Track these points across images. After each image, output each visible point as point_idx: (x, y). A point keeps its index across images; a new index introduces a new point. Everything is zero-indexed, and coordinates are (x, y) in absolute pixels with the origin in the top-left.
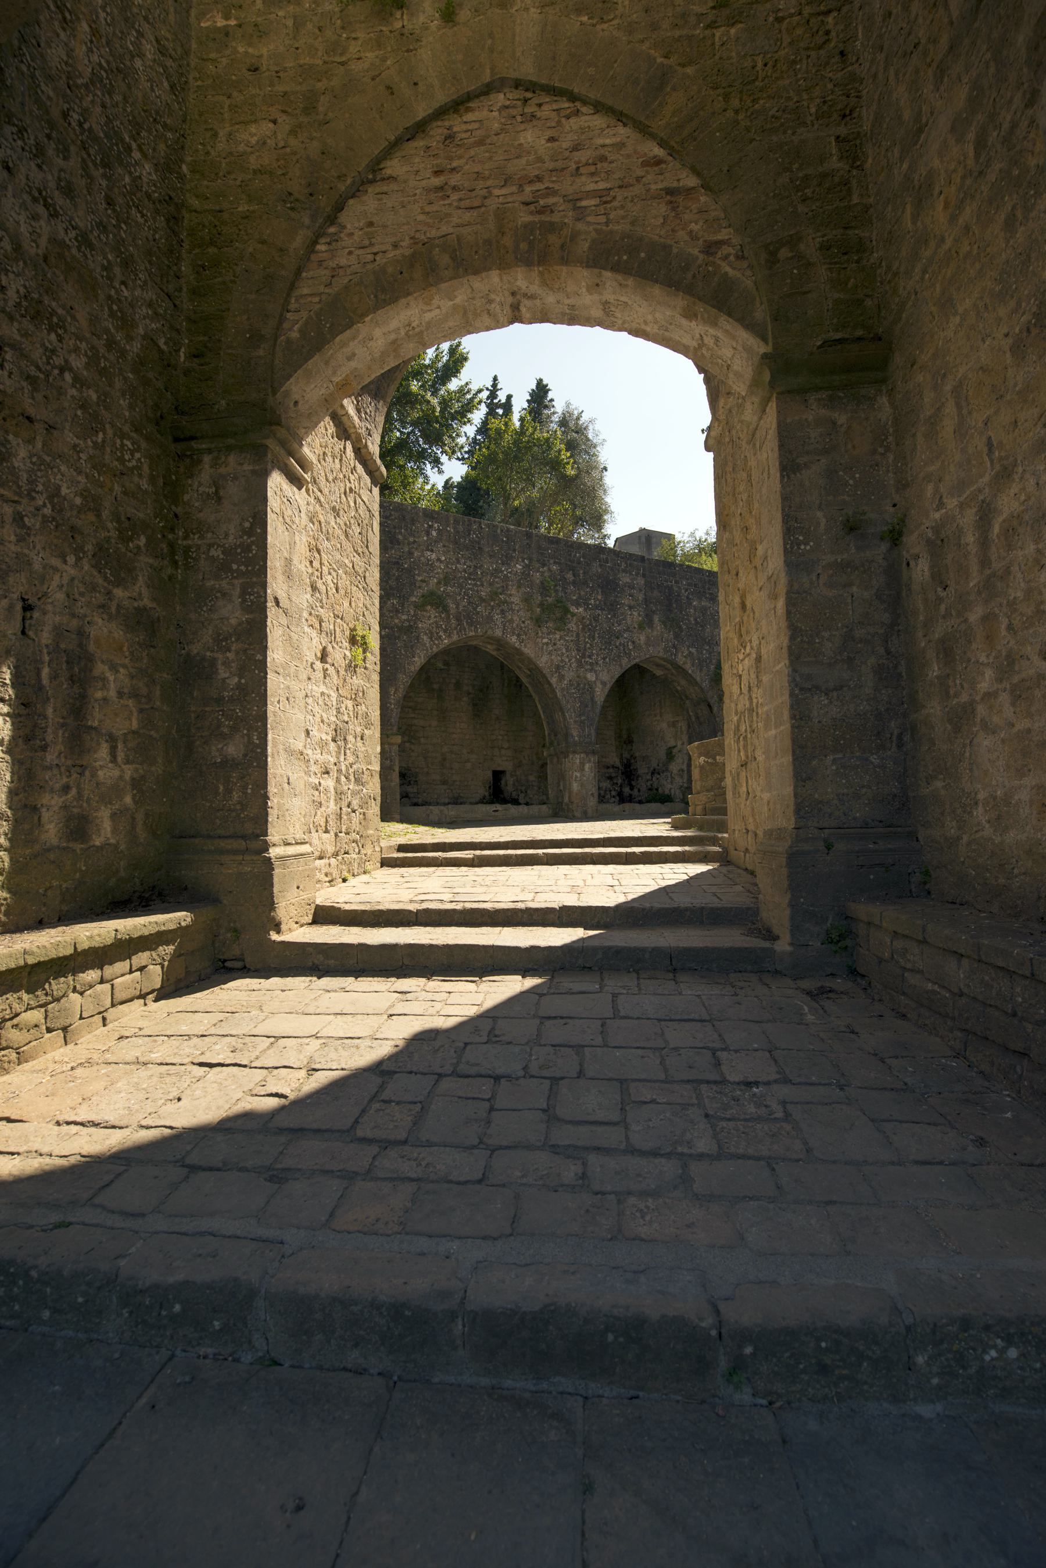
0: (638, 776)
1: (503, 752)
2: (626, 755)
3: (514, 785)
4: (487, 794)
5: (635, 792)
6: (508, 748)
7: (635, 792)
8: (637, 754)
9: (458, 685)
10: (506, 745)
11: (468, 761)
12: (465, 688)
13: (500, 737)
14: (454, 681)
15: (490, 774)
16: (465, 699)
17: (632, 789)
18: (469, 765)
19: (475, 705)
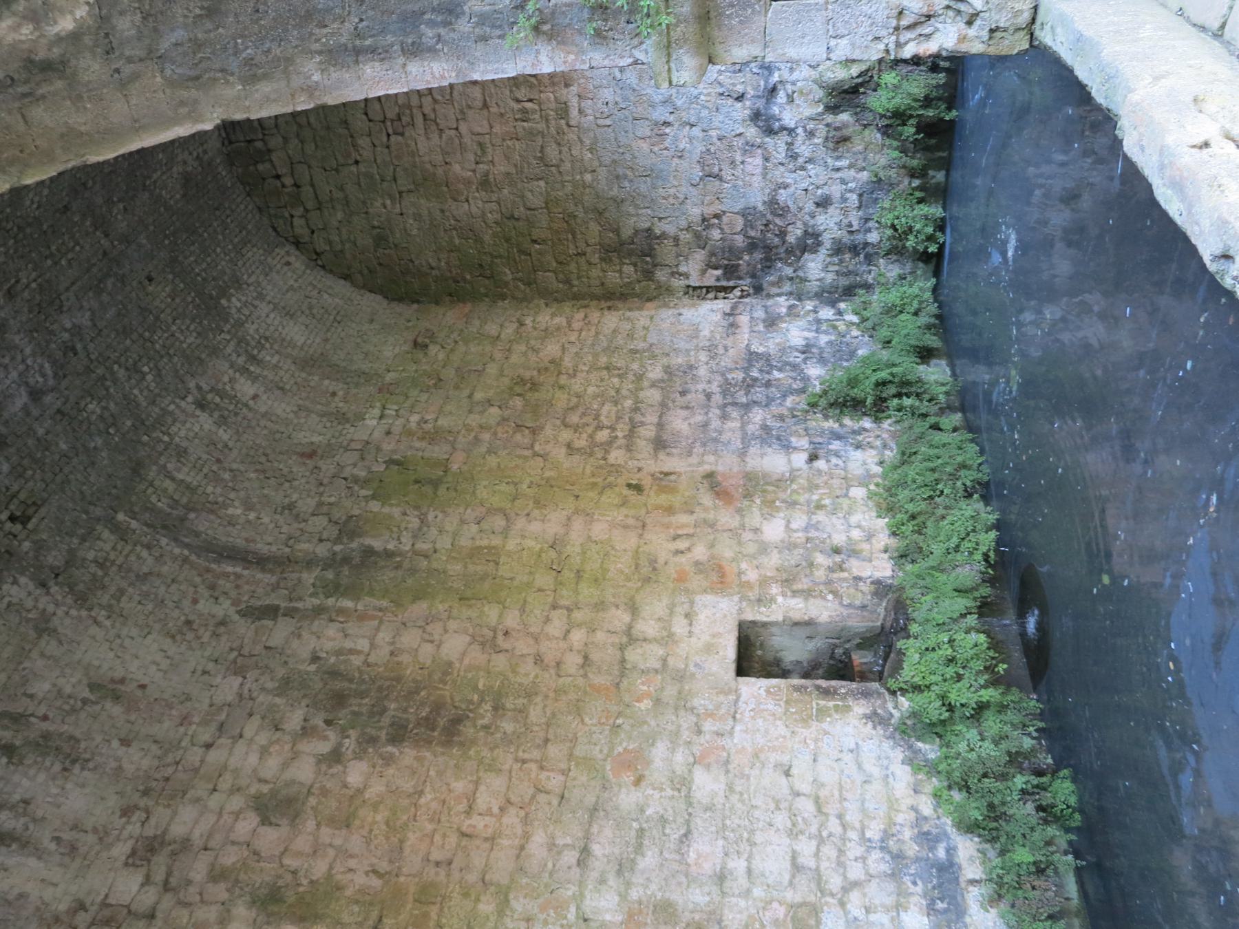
0: (772, 203)
1: (647, 627)
2: (694, 268)
3: (807, 594)
4: (860, 708)
5: (829, 224)
6: (634, 610)
7: (829, 224)
8: (695, 212)
9: (277, 806)
10: (620, 618)
11: (682, 784)
12: (304, 771)
13: (577, 637)
14: (246, 825)
15: (753, 687)
16: (356, 773)
17: (811, 240)
18: (706, 784)
19: (399, 734)
